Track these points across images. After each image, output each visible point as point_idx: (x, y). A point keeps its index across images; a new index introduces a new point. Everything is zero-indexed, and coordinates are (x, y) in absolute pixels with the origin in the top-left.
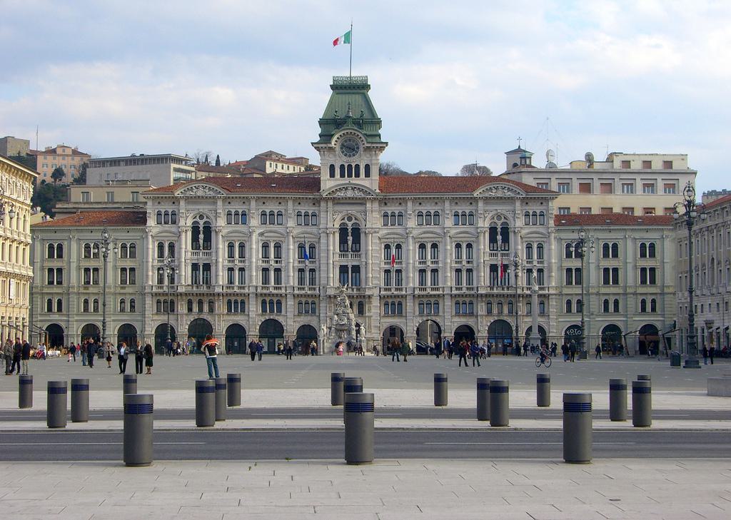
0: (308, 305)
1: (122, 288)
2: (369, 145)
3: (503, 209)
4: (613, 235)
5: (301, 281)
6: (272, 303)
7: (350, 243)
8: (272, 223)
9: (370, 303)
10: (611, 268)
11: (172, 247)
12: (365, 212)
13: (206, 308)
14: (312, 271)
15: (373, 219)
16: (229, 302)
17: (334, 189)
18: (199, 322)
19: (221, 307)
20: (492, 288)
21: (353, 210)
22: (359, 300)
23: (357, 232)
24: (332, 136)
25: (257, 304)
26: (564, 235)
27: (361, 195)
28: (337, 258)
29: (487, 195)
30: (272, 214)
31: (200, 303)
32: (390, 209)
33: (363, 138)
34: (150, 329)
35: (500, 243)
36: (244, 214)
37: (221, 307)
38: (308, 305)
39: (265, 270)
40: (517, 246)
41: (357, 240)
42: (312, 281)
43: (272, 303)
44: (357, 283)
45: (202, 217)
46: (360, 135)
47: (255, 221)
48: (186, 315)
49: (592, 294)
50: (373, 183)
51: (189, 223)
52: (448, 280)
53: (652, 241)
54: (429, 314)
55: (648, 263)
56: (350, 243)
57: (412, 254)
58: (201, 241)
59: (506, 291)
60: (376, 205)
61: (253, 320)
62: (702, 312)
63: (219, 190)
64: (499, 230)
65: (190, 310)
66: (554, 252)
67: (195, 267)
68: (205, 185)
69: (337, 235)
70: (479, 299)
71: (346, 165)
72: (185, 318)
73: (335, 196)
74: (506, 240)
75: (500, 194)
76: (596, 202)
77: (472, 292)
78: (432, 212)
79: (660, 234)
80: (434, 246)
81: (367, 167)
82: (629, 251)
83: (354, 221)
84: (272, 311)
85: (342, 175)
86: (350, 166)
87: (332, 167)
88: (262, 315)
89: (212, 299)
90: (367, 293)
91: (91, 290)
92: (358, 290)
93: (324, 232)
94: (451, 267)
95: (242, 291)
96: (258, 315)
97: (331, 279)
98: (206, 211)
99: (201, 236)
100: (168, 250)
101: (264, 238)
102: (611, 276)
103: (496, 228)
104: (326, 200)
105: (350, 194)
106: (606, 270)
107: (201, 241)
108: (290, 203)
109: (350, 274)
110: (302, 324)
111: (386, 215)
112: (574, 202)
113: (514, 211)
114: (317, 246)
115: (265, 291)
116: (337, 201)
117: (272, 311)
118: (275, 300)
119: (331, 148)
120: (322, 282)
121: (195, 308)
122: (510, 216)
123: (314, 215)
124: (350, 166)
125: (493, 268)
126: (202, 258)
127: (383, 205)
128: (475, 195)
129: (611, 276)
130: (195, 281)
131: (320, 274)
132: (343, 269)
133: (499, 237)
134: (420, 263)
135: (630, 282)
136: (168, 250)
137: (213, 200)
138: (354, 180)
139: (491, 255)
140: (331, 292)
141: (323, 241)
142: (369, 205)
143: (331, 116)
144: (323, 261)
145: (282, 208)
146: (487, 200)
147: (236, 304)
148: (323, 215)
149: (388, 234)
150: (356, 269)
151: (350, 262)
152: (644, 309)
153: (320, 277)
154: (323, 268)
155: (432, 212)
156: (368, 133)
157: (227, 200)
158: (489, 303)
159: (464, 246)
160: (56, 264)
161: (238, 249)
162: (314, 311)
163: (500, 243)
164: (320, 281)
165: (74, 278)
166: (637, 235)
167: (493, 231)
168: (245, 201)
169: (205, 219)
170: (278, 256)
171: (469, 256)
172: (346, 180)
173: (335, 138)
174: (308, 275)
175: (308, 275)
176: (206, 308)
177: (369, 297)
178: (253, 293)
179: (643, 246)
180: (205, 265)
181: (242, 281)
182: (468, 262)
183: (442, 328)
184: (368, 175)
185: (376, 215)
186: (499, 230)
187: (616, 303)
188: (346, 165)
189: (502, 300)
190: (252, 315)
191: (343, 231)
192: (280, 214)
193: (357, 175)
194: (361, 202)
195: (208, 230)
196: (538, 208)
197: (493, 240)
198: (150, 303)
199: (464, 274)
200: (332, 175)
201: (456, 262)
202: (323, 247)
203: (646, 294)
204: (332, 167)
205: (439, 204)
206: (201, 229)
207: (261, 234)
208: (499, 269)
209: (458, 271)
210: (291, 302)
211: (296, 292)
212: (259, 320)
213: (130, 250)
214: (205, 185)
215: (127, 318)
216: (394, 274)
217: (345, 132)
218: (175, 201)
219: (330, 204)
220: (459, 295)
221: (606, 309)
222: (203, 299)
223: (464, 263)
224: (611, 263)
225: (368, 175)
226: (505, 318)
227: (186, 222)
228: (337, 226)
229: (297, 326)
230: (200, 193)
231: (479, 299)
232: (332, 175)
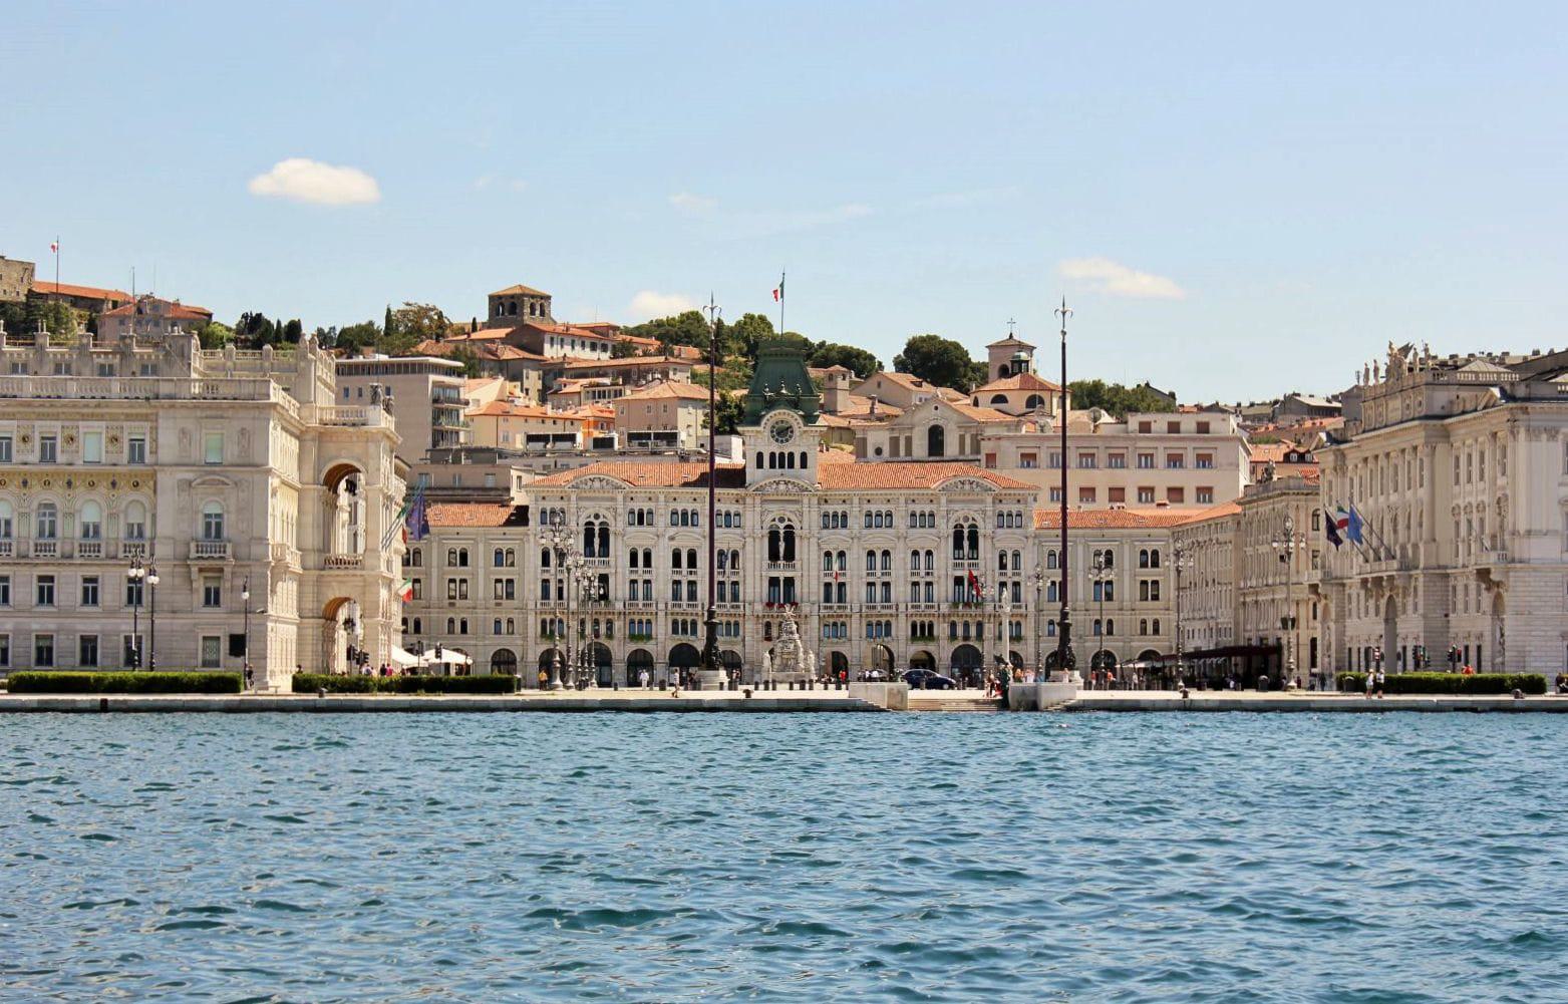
14: (735, 583)
15: (807, 523)
17: (763, 483)
39: (677, 583)
51: (583, 521)
57: (856, 562)
60: (815, 501)
64: (966, 534)
69: (766, 540)
74: (974, 545)
77: (932, 611)
81: (804, 456)
84: (685, 631)
85: (772, 466)
86: (782, 455)
87: (760, 456)
99: (597, 541)
113: (984, 512)
115: (677, 610)
117: (685, 631)
119: (758, 432)
125: (959, 581)
129: (1105, 591)
132: (774, 582)
133: (966, 544)
138: (786, 470)
141: (749, 548)
144: (749, 573)
151: (781, 574)
152: (1144, 632)
154: (749, 580)
171: (929, 567)
172: (778, 471)
182: (928, 574)
183: (895, 655)
186: (966, 534)
190: (661, 638)
191: (773, 537)
192: (694, 514)
193: (791, 466)
195: (605, 534)
197: (958, 545)
199: (922, 588)
200: (760, 465)
202: (749, 556)
207: (672, 538)
212: (670, 645)
216: (834, 592)
219: (758, 500)
226: (971, 643)
228: (766, 531)
231: (941, 619)
232: (760, 465)
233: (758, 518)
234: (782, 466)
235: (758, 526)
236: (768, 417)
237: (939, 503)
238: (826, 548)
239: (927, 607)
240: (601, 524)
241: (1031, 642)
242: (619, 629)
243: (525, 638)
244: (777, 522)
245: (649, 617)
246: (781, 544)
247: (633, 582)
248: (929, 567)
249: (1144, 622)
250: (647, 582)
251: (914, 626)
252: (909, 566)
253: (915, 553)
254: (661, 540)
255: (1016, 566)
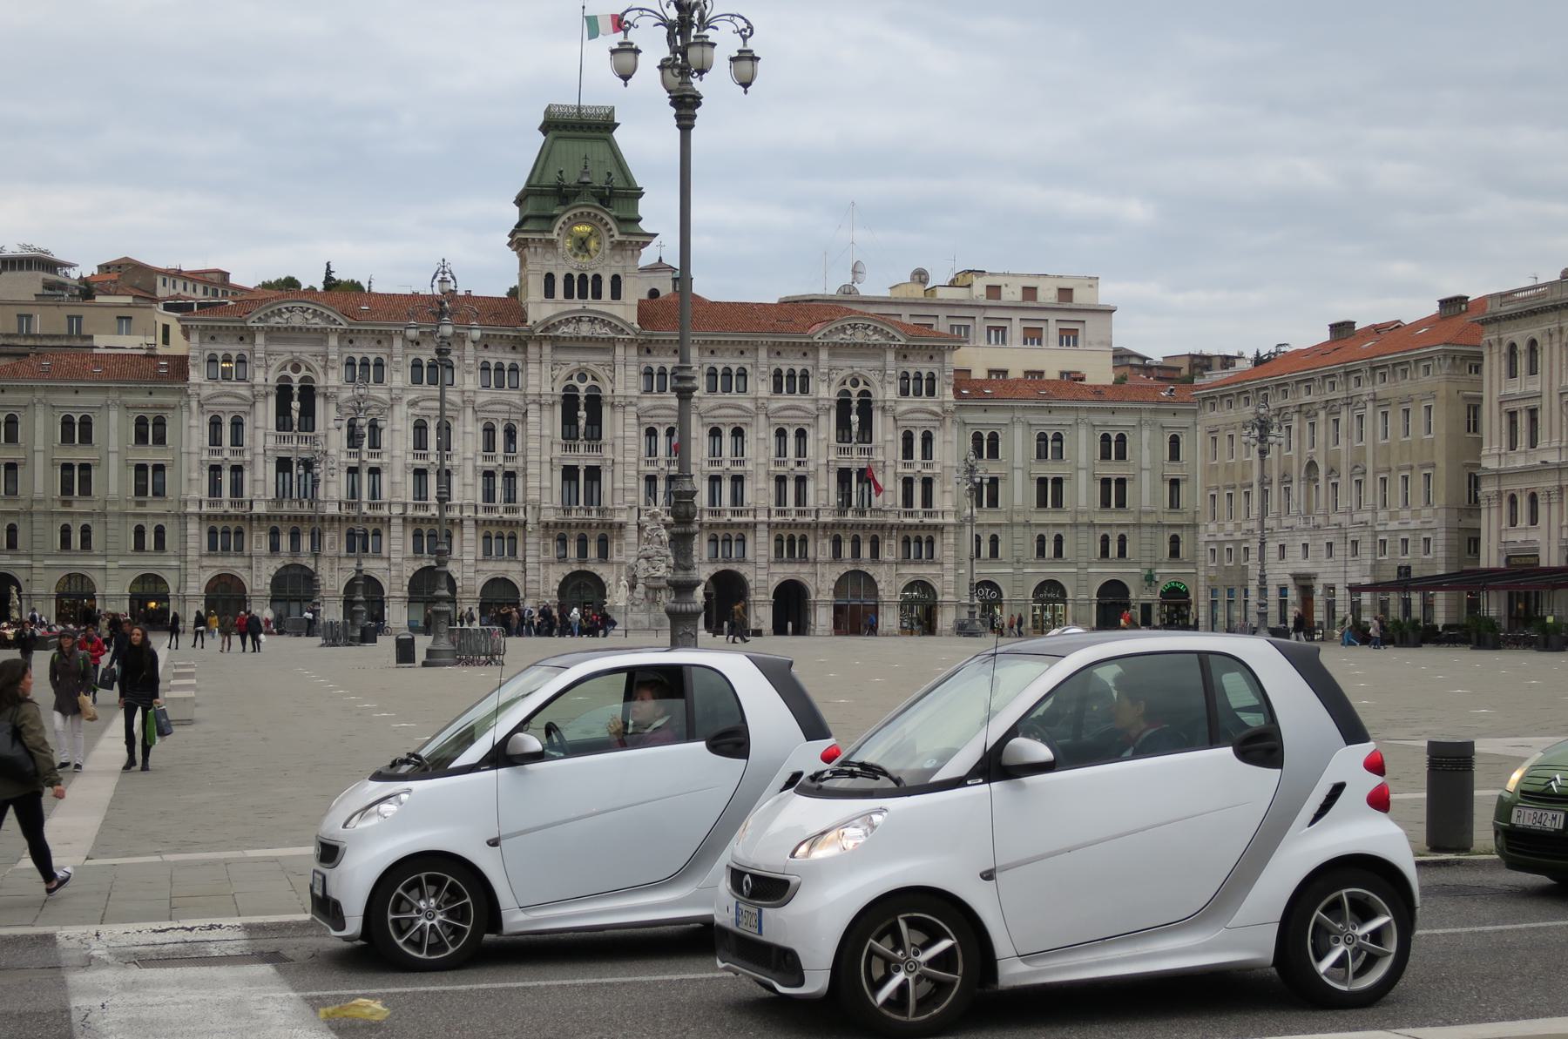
0: (502, 537)
1: (139, 504)
2: (623, 238)
3: (863, 366)
4: (1056, 418)
5: (489, 495)
6: (433, 536)
7: (582, 423)
8: (500, 386)
9: (621, 537)
10: (1050, 477)
11: (237, 424)
12: (612, 366)
13: (866, 551)
15: (623, 379)
16: (351, 534)
17: (555, 321)
18: (292, 571)
19: (334, 542)
20: (842, 512)
21: (592, 361)
22: (600, 532)
23: (595, 403)
24: (552, 218)
25: (404, 538)
26: (970, 417)
27: (604, 332)
28: (558, 451)
29: (836, 339)
30: (727, 373)
31: (295, 536)
32: (656, 362)
33: (612, 225)
34: (196, 585)
35: (855, 428)
36: (379, 364)
37: (334, 542)
38: (502, 537)
40: (885, 432)
41: (595, 420)
42: (510, 497)
43: (433, 536)
44: (593, 498)
45: (855, 383)
46: (607, 219)
47: (399, 378)
48: (267, 557)
49: (1018, 524)
50: (626, 311)
51: (273, 380)
52: (759, 493)
53: (1121, 430)
54: (728, 559)
55: (1113, 470)
56: (582, 423)
58: (295, 415)
59: (868, 518)
60: (633, 351)
61: (395, 564)
62: (1282, 557)
63: (333, 316)
64: (855, 404)
65: (275, 547)
66: (950, 449)
67: (283, 465)
68: (305, 305)
70: (820, 532)
71: (576, 275)
72: (265, 563)
73: (558, 333)
75: (859, 338)
76: (1016, 359)
77: (808, 519)
78: (734, 369)
79: (1137, 417)
80: (738, 433)
82: (1082, 447)
83: (590, 382)
85: (568, 294)
86: (583, 277)
87: (550, 278)
88: (415, 559)
89: (317, 525)
90: (620, 518)
91: (77, 507)
92: (599, 511)
93: (534, 402)
94: (768, 473)
95: (378, 513)
96: (408, 559)
97: (542, 490)
98: (306, 357)
99: (296, 405)
100: (226, 429)
101: (417, 411)
102: (1049, 492)
103: (850, 402)
104: (540, 341)
105: (585, 330)
106: (1042, 482)
107: (295, 415)
108: (763, 354)
109: (582, 481)
110: (491, 575)
111: (648, 373)
112: (978, 358)
113: (883, 371)
114: (519, 428)
115: (421, 514)
116: (558, 343)
118: (734, 534)
120: (530, 497)
121: (285, 542)
122: (875, 378)
123: (514, 369)
124: (583, 277)
126: (296, 447)
127: (644, 352)
128: (816, 339)
129: (1049, 492)
130: (281, 495)
131: (526, 482)
132: (569, 473)
133: (855, 418)
134: (711, 463)
135: (1082, 502)
136: (226, 429)
137: (321, 336)
138: (592, 305)
139: (840, 451)
140: (550, 516)
141: (532, 418)
142: (619, 351)
143: (551, 178)
145: (745, 361)
146: (835, 349)
147: (362, 536)
148: (532, 368)
149: (655, 408)
150: (594, 473)
151: (582, 458)
153: (525, 488)
154: (532, 470)
155: (734, 369)
156: (622, 215)
157: (348, 337)
158: (837, 542)
159: (791, 433)
160: (78, 455)
161: (363, 433)
162: (513, 552)
163: (855, 428)
164: (525, 494)
165: (113, 481)
166: (1097, 419)
167: (843, 406)
168: (383, 338)
169: (303, 372)
170: (445, 446)
172: (576, 304)
173: (559, 224)
174: (501, 482)
175: (501, 482)
176: (305, 542)
177: (621, 526)
178: (397, 517)
179: (1106, 438)
180: (861, 472)
181: (375, 493)
182: (799, 463)
184: (616, 294)
185: (633, 371)
186: (855, 404)
187: (1059, 540)
188: (576, 275)
189: (840, 533)
191: (569, 402)
193: (597, 295)
194: (607, 345)
195: (308, 393)
196: (925, 368)
198: (196, 535)
200: (549, 292)
201: (777, 463)
203: (1110, 525)
204: (550, 278)
205: (747, 354)
206: (296, 390)
207: (413, 404)
208: (854, 477)
209: (781, 480)
210: (469, 532)
211: (481, 515)
212: (410, 568)
213: (150, 430)
214: (305, 305)
215: (150, 562)
217: (577, 211)
218: (245, 335)
219: (547, 349)
220: (783, 524)
221: (1041, 552)
222: (296, 526)
223: (792, 464)
224: (1050, 470)
225: (616, 294)
226: (863, 568)
227: (264, 377)
228: (559, 391)
229: (481, 581)
230: (297, 320)
231: (820, 532)
233: (547, 369)
234: (583, 295)
235: (547, 389)
236: (564, 218)
237: (817, 359)
238: (652, 422)
239: (799, 513)
240: (303, 379)
241: (949, 565)
242: (332, 543)
243: (182, 556)
244: (575, 381)
245: (378, 526)
246: (582, 413)
247: (353, 471)
248: (801, 451)
249: (1105, 540)
250: (375, 471)
251: (779, 539)
252: (773, 452)
253: (781, 433)
254: (396, 408)
255: (927, 453)
